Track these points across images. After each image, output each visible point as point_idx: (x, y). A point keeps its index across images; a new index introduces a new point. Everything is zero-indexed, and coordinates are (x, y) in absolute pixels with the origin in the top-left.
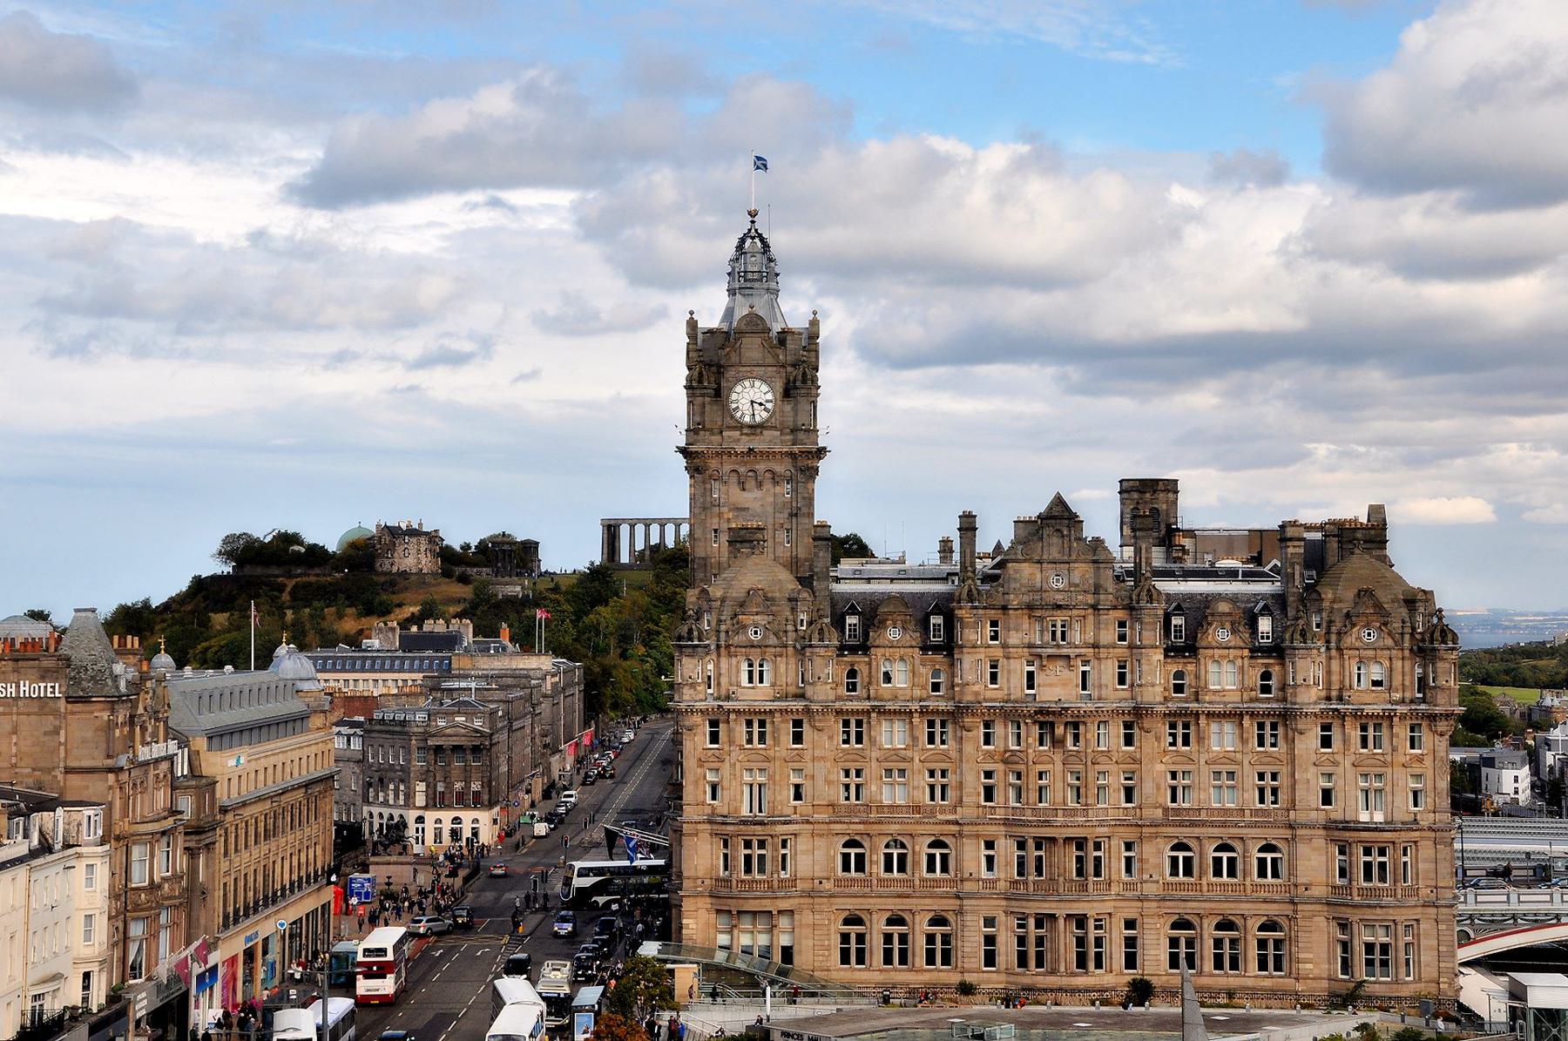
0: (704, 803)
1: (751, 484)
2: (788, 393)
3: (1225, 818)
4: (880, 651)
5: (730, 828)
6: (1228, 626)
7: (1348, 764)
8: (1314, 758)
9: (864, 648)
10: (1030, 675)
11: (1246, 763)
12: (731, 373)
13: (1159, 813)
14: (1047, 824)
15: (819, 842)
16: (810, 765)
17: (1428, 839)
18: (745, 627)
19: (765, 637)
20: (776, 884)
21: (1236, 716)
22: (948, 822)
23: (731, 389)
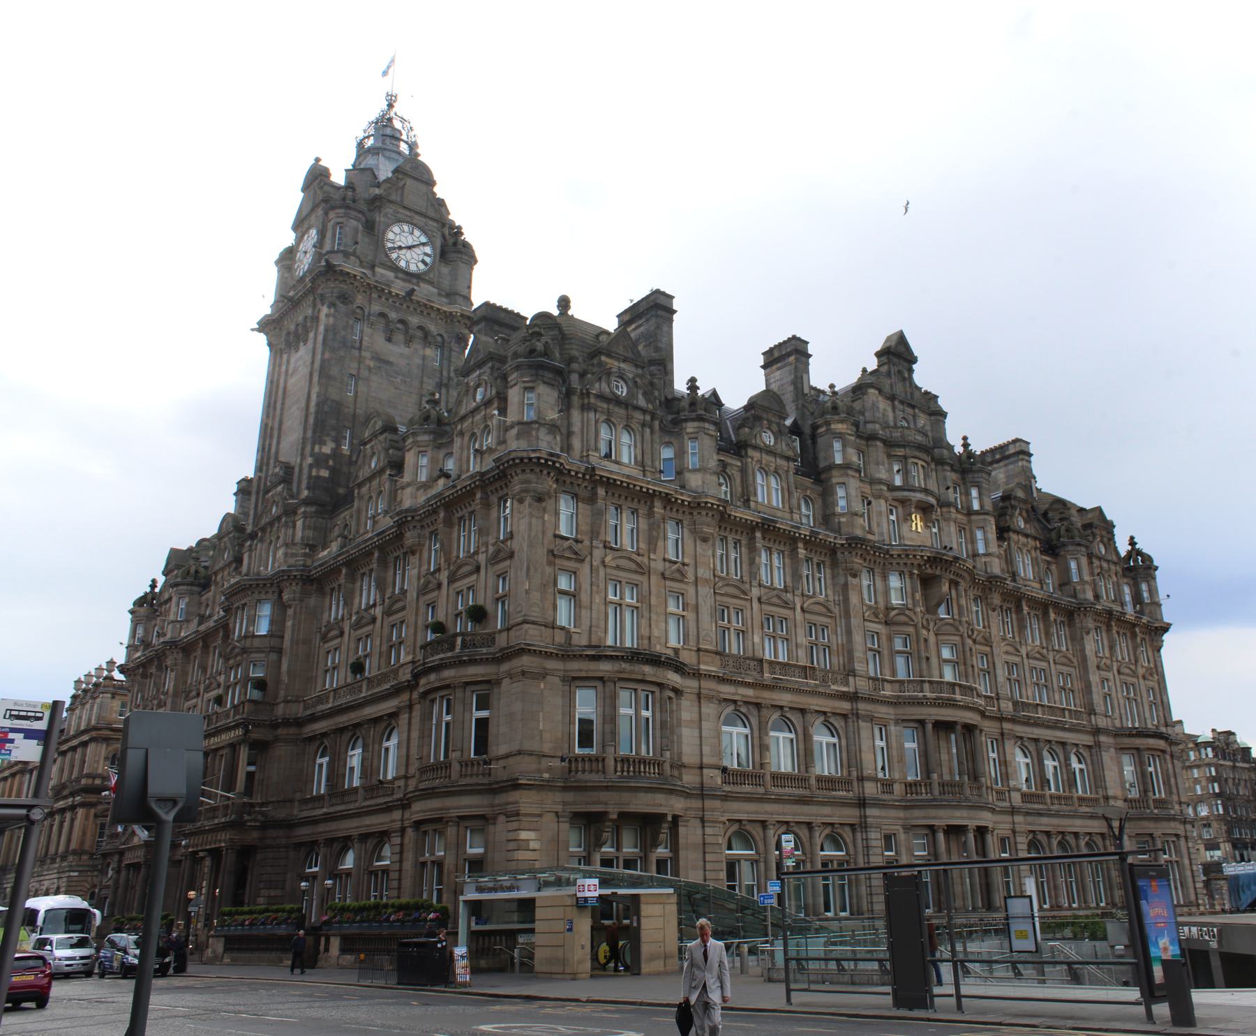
0: (553, 626)
1: (399, 337)
4: (756, 455)
12: (389, 210)
14: (952, 704)
15: (709, 709)
16: (691, 590)
18: (609, 374)
20: (667, 767)
21: (1043, 607)
22: (843, 696)
23: (388, 226)
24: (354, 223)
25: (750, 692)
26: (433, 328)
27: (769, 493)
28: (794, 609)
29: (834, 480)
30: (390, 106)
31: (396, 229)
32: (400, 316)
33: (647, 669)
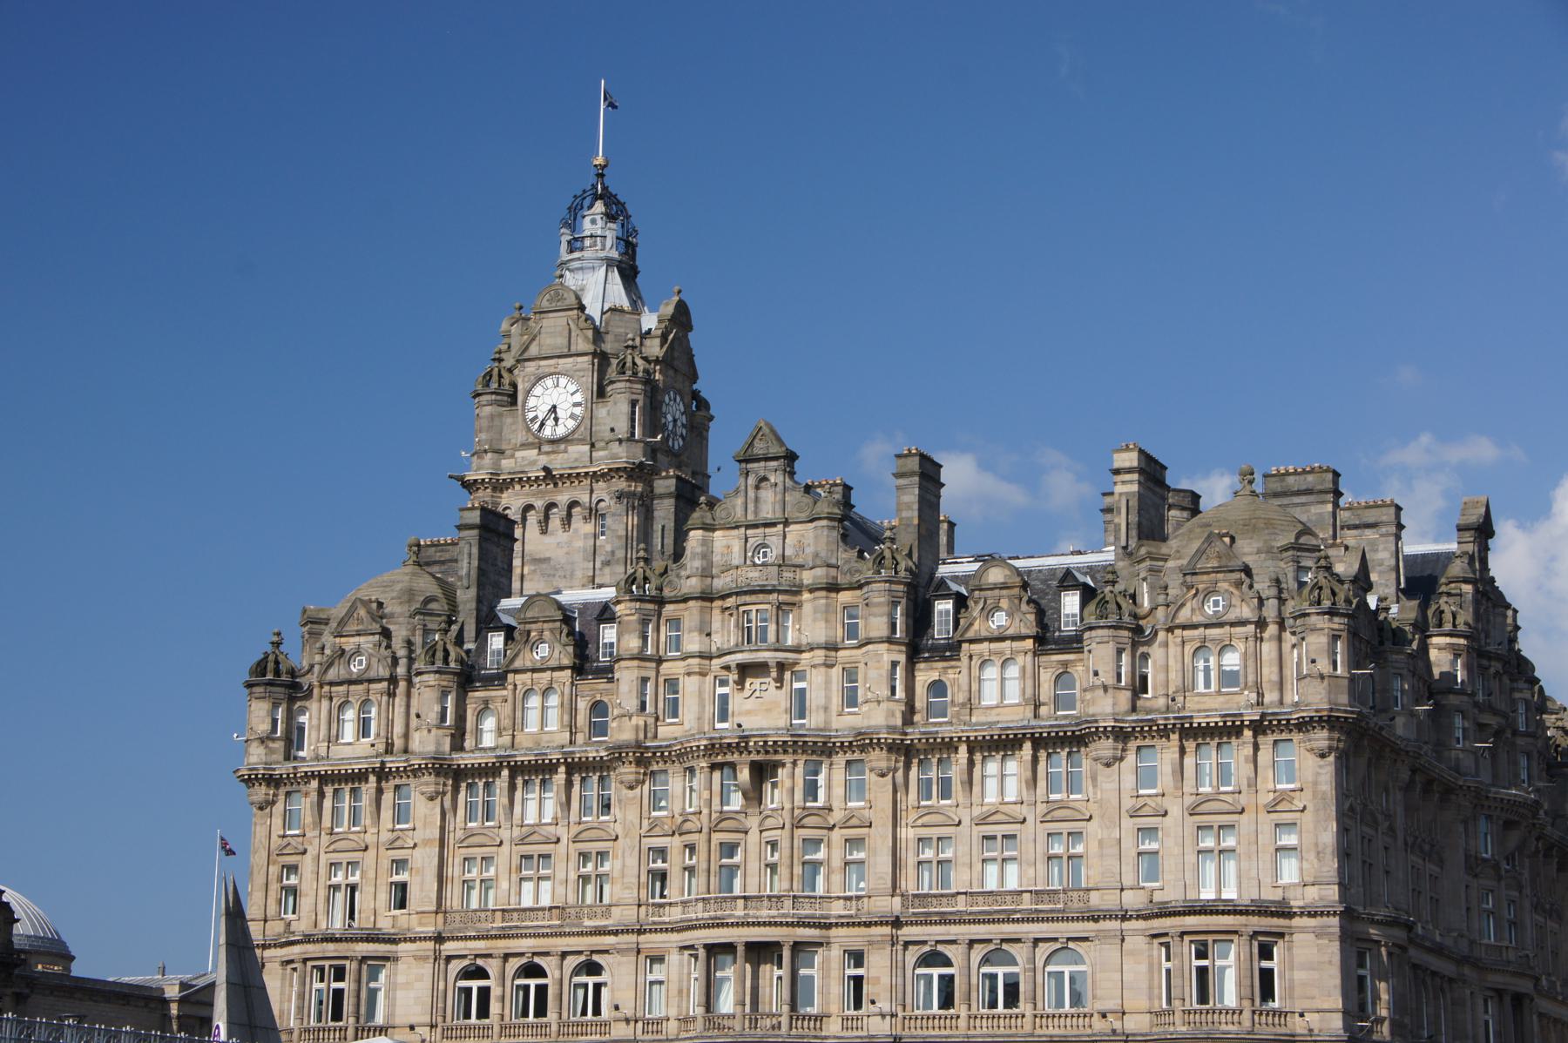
2: (601, 393)
3: (999, 908)
5: (297, 949)
6: (1004, 603)
7: (1175, 810)
8: (1128, 803)
9: (500, 679)
10: (724, 699)
11: (1030, 820)
12: (531, 367)
13: (897, 900)
17: (1303, 930)
19: (369, 666)
24: (488, 409)
25: (481, 946)
26: (584, 498)
27: (542, 718)
28: (558, 840)
29: (617, 676)
30: (602, 175)
31: (538, 390)
32: (548, 499)
33: (331, 946)
